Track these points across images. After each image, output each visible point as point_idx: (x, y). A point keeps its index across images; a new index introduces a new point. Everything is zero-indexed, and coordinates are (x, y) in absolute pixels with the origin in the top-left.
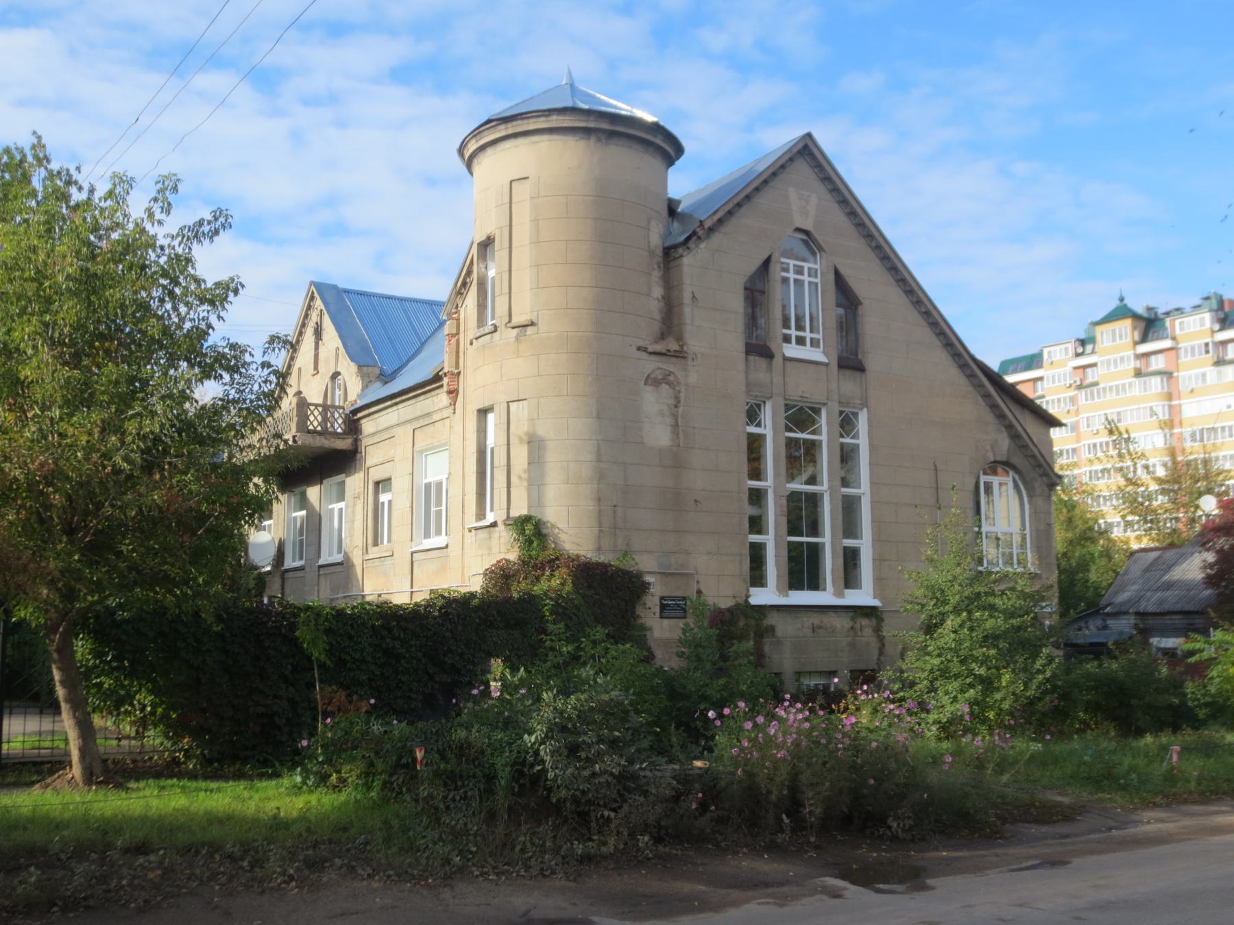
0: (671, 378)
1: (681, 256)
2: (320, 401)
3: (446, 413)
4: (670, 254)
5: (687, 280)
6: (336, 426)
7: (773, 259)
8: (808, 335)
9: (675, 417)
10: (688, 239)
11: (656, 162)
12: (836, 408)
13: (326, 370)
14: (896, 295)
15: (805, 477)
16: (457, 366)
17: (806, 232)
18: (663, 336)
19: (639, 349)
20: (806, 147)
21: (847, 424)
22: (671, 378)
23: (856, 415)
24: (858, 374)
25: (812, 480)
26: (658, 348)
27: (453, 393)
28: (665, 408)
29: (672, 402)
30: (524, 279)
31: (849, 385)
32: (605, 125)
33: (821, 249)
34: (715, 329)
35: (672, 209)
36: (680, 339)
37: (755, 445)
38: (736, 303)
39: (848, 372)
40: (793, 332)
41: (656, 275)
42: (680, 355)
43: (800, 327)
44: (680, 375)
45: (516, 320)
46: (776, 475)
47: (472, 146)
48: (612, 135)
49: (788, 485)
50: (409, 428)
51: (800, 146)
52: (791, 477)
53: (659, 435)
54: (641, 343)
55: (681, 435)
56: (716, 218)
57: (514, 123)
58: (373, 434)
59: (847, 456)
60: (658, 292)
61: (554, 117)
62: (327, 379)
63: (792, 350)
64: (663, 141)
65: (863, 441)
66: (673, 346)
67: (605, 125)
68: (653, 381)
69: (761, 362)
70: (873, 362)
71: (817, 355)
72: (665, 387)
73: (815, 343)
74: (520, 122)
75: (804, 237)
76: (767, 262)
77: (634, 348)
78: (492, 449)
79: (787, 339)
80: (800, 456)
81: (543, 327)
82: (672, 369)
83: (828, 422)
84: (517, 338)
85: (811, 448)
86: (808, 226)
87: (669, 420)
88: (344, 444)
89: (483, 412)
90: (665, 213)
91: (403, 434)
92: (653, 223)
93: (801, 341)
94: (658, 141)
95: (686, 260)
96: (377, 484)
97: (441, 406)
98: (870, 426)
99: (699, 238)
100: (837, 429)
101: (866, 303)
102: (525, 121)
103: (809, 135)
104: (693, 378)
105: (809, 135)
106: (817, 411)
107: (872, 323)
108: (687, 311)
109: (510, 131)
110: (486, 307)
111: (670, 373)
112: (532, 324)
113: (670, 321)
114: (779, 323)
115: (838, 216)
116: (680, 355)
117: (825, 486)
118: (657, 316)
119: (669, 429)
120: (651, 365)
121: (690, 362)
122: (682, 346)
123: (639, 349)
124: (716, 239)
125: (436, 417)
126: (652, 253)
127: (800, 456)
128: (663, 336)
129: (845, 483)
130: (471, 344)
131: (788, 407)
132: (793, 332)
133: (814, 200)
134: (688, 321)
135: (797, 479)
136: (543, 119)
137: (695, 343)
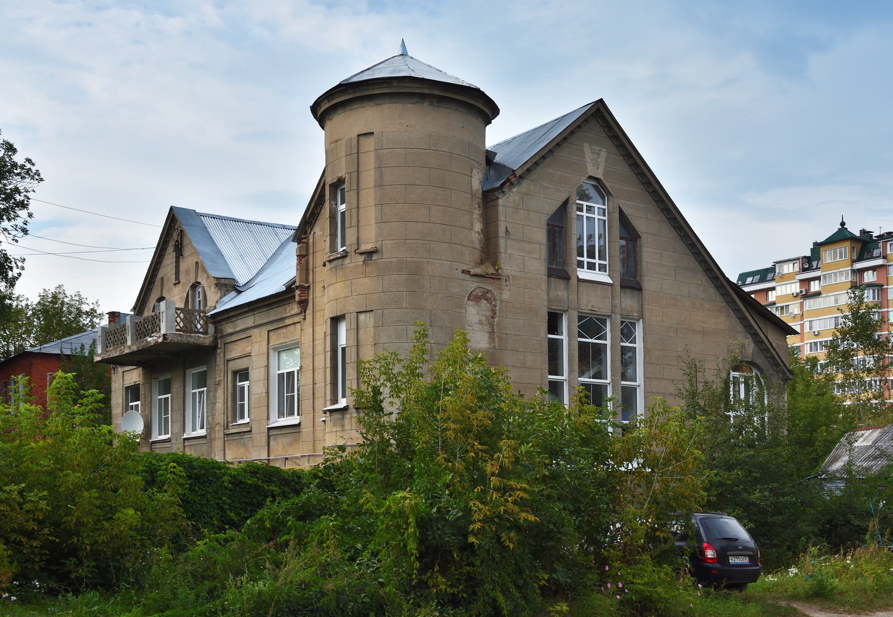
0: (489, 295)
1: (498, 198)
2: (182, 306)
3: (297, 319)
4: (489, 198)
5: (502, 217)
7: (570, 202)
8: (597, 261)
9: (492, 325)
10: (503, 185)
11: (477, 122)
12: (618, 319)
13: (187, 280)
14: (667, 230)
15: (592, 373)
16: (307, 281)
17: (597, 180)
18: (482, 262)
19: (463, 272)
20: (598, 110)
21: (627, 332)
22: (489, 295)
23: (634, 325)
24: (636, 293)
25: (598, 375)
26: (478, 271)
27: (304, 304)
28: (483, 318)
29: (489, 314)
31: (628, 302)
32: (437, 92)
33: (609, 193)
34: (524, 258)
35: (489, 156)
36: (494, 264)
37: (554, 348)
38: (541, 235)
39: (628, 291)
40: (585, 259)
41: (477, 213)
42: (496, 277)
43: (591, 255)
44: (495, 292)
45: (365, 247)
46: (571, 371)
48: (442, 100)
49: (580, 379)
50: (264, 331)
51: (594, 110)
52: (582, 373)
54: (465, 268)
55: (496, 340)
56: (525, 168)
58: (231, 334)
59: (626, 359)
60: (478, 227)
62: (188, 288)
63: (584, 274)
65: (639, 345)
66: (491, 270)
68: (475, 298)
69: (561, 284)
70: (650, 283)
71: (604, 278)
72: (484, 302)
73: (602, 268)
75: (595, 183)
76: (566, 203)
77: (460, 271)
78: (344, 349)
79: (580, 264)
80: (590, 357)
83: (611, 331)
85: (599, 350)
86: (599, 174)
87: (487, 328)
89: (336, 321)
90: (484, 162)
91: (259, 335)
92: (475, 171)
93: (591, 267)
95: (501, 202)
96: (235, 373)
97: (293, 312)
98: (644, 333)
99: (512, 184)
100: (618, 334)
101: (643, 236)
103: (601, 101)
104: (506, 295)
105: (601, 101)
106: (604, 322)
107: (649, 254)
108: (502, 242)
109: (358, 95)
110: (336, 236)
111: (488, 291)
113: (489, 250)
114: (575, 252)
115: (623, 168)
116: (496, 277)
117: (609, 380)
118: (478, 246)
119: (487, 335)
120: (472, 285)
121: (504, 283)
122: (497, 271)
123: (463, 272)
124: (525, 184)
125: (288, 322)
126: (473, 195)
127: (590, 357)
128: (482, 262)
129: (624, 377)
130: (324, 265)
131: (580, 318)
132: (585, 259)
133: (604, 154)
134: (502, 250)
135: (587, 374)
137: (508, 267)
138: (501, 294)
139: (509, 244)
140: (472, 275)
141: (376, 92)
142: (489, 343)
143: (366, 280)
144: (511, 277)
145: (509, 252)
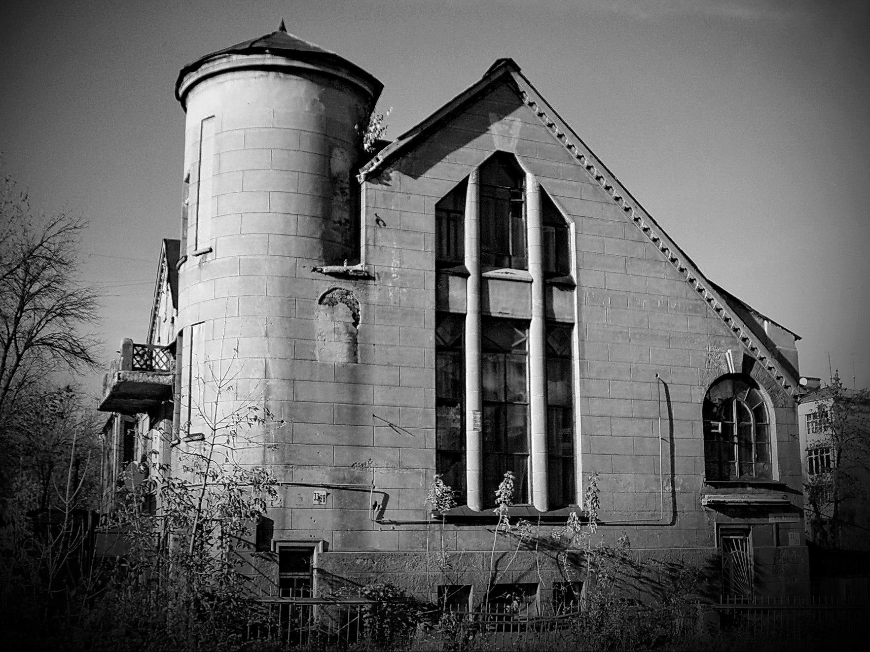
6: (161, 364)
28: (340, 326)
30: (207, 208)
38: (427, 223)
45: (201, 249)
47: (181, 93)
53: (335, 351)
55: (359, 353)
57: (203, 67)
61: (234, 57)
64: (349, 74)
67: (281, 61)
74: (206, 65)
81: (219, 252)
82: (351, 288)
84: (200, 265)
87: (345, 338)
88: (166, 380)
92: (337, 151)
94: (343, 74)
102: (211, 64)
112: (211, 250)
136: (225, 60)
139: (379, 234)
140: (326, 274)
141: (216, 69)
143: (200, 286)
144: (383, 275)
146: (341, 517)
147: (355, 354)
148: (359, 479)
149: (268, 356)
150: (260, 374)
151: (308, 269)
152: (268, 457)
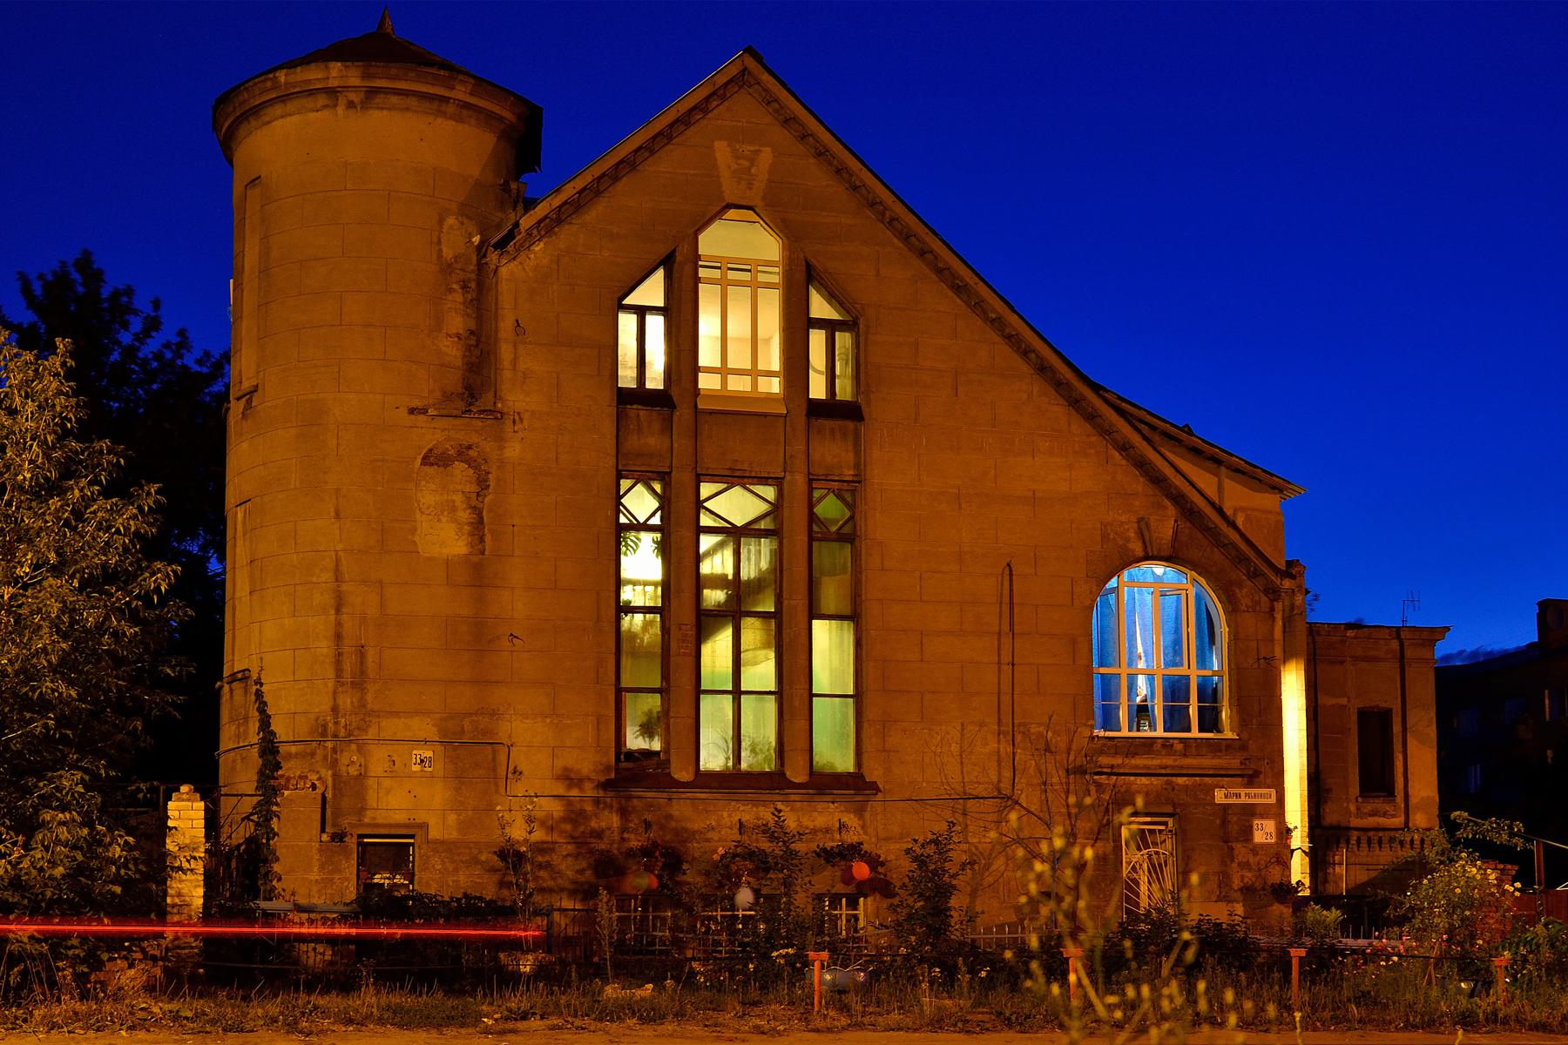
0: (472, 453)
5: (506, 300)
9: (478, 512)
19: (412, 411)
22: (472, 453)
28: (458, 499)
29: (474, 488)
44: (488, 447)
55: (488, 538)
60: (457, 323)
72: (459, 468)
87: (464, 515)
104: (513, 450)
108: (506, 352)
120: (433, 433)
123: (412, 411)
138: (501, 448)
142: (471, 545)
144: (526, 416)
145: (522, 366)
146: (457, 790)
147: (482, 540)
148: (485, 732)
149: (340, 547)
150: (327, 576)
151: (403, 412)
152: (340, 702)
